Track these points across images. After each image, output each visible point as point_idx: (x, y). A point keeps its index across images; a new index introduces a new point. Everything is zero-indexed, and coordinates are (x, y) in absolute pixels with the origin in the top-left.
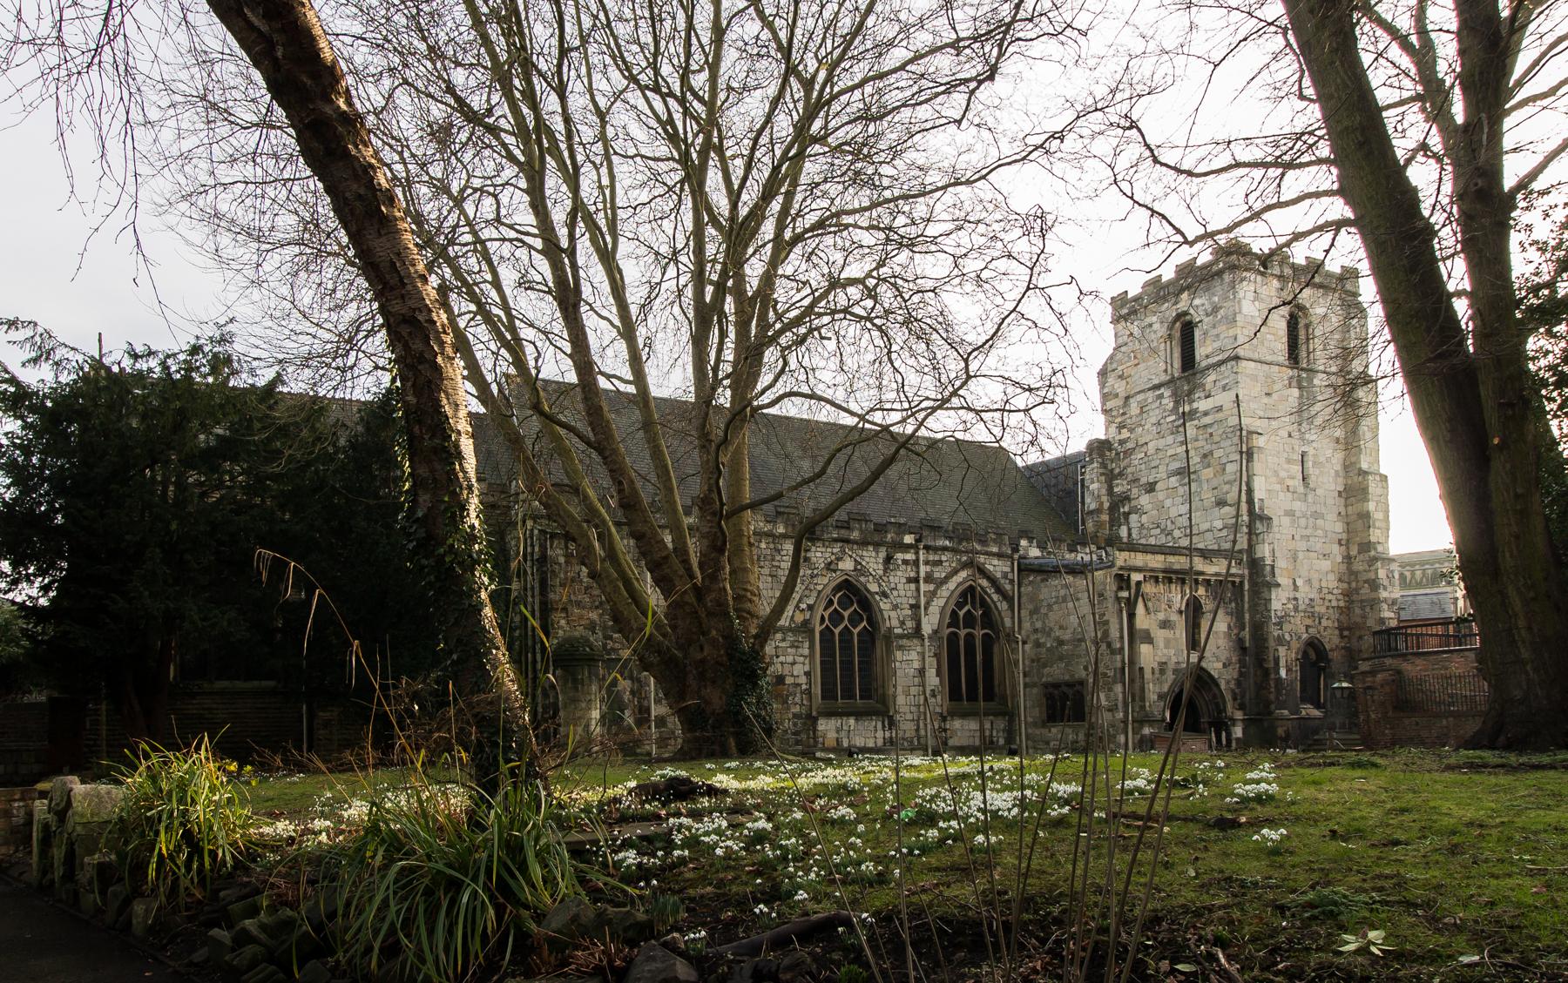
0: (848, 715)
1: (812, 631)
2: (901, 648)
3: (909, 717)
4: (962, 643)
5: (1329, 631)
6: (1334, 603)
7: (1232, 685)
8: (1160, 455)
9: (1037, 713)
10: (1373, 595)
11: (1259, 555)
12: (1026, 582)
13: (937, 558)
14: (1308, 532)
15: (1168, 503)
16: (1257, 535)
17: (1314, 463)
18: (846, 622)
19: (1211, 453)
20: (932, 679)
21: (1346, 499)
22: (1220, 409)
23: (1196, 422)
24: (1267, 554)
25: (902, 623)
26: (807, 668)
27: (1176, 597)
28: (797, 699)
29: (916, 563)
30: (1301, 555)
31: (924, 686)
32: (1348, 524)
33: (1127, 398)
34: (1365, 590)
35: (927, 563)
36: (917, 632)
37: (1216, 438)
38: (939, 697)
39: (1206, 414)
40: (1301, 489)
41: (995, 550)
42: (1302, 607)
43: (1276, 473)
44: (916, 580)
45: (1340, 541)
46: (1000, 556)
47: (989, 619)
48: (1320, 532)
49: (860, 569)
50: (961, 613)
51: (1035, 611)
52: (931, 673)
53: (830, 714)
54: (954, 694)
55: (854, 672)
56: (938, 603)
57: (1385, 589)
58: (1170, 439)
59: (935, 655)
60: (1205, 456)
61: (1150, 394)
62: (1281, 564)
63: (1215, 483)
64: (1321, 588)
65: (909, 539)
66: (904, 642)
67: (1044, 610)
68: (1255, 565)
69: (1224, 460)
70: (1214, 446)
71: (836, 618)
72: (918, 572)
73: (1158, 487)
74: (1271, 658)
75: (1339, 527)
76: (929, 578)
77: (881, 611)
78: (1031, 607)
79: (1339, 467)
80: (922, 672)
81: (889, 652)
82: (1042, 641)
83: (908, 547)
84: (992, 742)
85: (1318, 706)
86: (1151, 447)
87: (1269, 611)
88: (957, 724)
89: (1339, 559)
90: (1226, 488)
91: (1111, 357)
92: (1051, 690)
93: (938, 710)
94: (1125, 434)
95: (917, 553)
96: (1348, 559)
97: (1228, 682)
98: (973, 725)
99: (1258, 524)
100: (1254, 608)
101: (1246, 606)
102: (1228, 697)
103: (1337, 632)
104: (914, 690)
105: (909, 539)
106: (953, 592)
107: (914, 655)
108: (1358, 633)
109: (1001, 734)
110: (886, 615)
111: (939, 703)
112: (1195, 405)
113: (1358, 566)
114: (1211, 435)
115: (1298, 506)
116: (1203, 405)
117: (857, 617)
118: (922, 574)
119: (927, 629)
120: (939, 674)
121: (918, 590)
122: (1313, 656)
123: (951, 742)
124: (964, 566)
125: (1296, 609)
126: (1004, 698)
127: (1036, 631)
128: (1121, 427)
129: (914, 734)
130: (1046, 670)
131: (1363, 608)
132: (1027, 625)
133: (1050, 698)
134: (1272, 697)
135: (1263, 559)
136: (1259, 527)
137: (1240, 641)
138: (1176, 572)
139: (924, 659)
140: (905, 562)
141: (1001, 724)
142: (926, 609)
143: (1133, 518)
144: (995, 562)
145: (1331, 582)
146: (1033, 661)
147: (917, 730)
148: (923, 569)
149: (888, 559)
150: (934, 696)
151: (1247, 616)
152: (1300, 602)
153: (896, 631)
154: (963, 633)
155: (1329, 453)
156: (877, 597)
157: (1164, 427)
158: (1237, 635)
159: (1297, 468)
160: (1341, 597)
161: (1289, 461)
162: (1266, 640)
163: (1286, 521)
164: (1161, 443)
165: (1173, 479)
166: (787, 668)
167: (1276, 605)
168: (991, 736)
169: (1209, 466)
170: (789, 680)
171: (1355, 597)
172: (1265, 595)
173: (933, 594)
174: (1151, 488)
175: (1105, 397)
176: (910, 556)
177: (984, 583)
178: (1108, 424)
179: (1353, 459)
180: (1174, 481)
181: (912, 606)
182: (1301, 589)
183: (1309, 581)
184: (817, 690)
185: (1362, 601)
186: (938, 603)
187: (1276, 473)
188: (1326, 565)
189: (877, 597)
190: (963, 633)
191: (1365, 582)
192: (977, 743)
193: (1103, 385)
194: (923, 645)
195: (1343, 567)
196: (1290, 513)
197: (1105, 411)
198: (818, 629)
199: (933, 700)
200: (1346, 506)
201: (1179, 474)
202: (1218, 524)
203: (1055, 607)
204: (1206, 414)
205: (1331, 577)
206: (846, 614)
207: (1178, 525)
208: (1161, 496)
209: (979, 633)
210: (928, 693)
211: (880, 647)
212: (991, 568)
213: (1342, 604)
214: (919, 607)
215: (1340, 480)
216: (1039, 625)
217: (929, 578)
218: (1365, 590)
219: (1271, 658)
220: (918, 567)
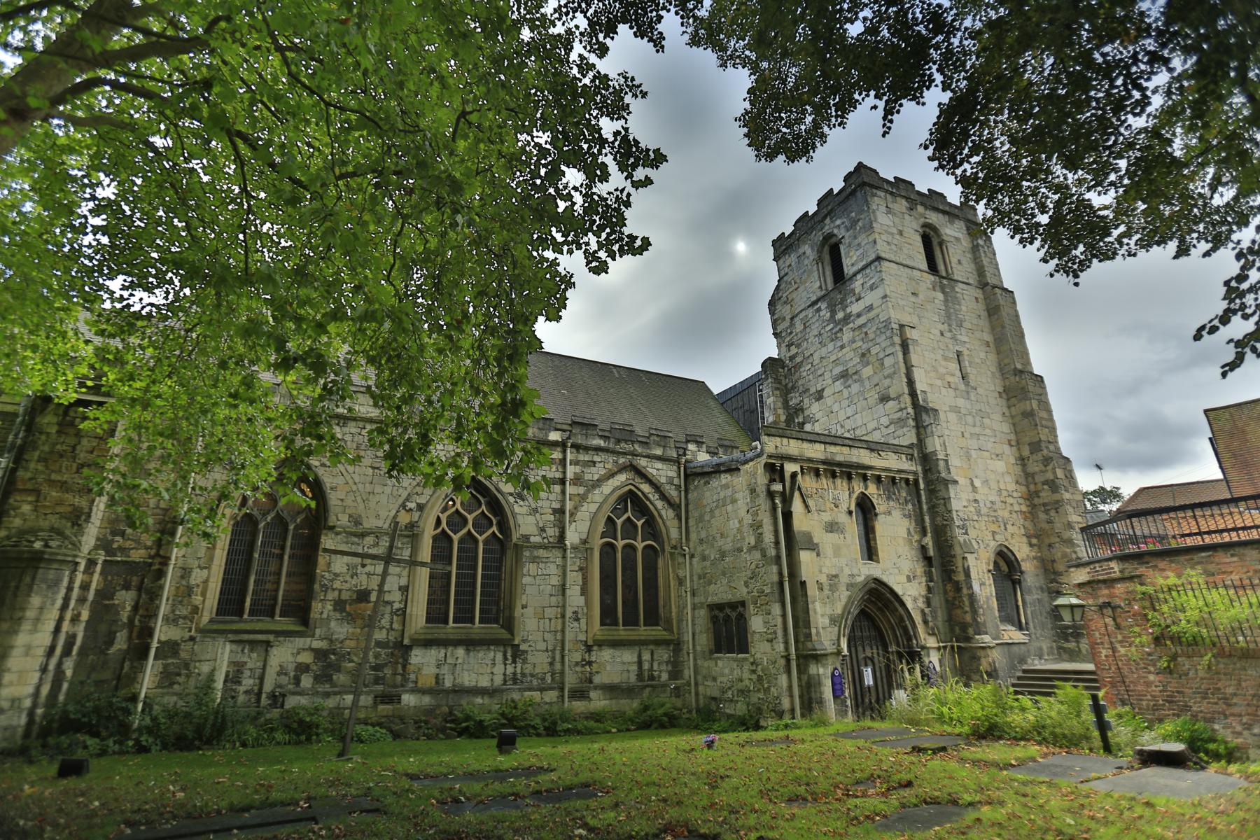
2: (535, 560)
3: (542, 646)
4: (619, 555)
5: (1017, 538)
6: (1016, 508)
7: (921, 604)
8: (825, 362)
9: (704, 640)
10: (1056, 497)
11: (930, 449)
12: (692, 487)
13: (587, 458)
14: (977, 430)
15: (836, 408)
16: (925, 428)
17: (970, 363)
18: (470, 526)
19: (869, 350)
20: (575, 598)
21: (1008, 400)
22: (870, 308)
23: (851, 325)
24: (938, 448)
25: (543, 530)
27: (843, 494)
29: (563, 462)
30: (973, 453)
31: (564, 606)
32: (1014, 425)
33: (792, 319)
34: (1046, 495)
35: (575, 463)
37: (871, 336)
38: (583, 621)
39: (859, 315)
40: (962, 387)
42: (984, 511)
43: (935, 369)
44: (562, 482)
45: (1009, 441)
47: (652, 528)
48: (988, 431)
50: (619, 522)
51: (700, 519)
54: (608, 616)
55: (474, 585)
56: (588, 509)
57: (1067, 491)
58: (831, 346)
59: (581, 569)
60: (863, 355)
61: (810, 312)
62: (955, 462)
63: (876, 380)
64: (1000, 490)
66: (541, 552)
67: (707, 518)
68: (927, 460)
69: (881, 355)
70: (871, 344)
72: (564, 473)
73: (826, 394)
74: (960, 569)
75: (1006, 428)
76: (577, 480)
77: (513, 513)
78: (696, 514)
79: (993, 369)
80: (563, 588)
82: (707, 552)
84: (652, 678)
85: (1021, 629)
86: (816, 356)
87: (950, 511)
88: (605, 655)
89: (1012, 461)
90: (887, 382)
91: (777, 288)
92: (716, 612)
93: (582, 637)
94: (794, 350)
95: (564, 452)
96: (1022, 460)
97: (915, 600)
98: (629, 656)
99: (924, 417)
100: (933, 508)
101: (925, 507)
102: (918, 618)
103: (1025, 539)
104: (550, 613)
105: (554, 436)
106: (607, 497)
107: (553, 569)
108: (1047, 541)
109: (664, 667)
110: (520, 519)
112: (848, 310)
113: (1034, 467)
114: (866, 333)
115: (961, 402)
116: (855, 308)
117: (484, 522)
118: (570, 475)
119: (572, 537)
120: (584, 591)
121: (563, 492)
122: (1005, 568)
123: (597, 680)
124: (622, 469)
125: (979, 513)
126: (669, 621)
127: (701, 541)
128: (789, 346)
129: (547, 668)
130: (712, 588)
131: (1047, 512)
132: (693, 536)
133: (714, 620)
134: (968, 618)
135: (934, 453)
136: (926, 419)
137: (923, 549)
138: (840, 464)
139: (564, 575)
141: (664, 654)
142: (572, 515)
145: (1009, 484)
146: (700, 578)
147: (551, 664)
148: (571, 471)
150: (577, 619)
151: (927, 518)
152: (982, 505)
153: (532, 539)
154: (620, 544)
155: (982, 355)
156: (511, 499)
157: (825, 335)
158: (919, 541)
159: (954, 366)
160: (1021, 501)
161: (946, 358)
162: (951, 546)
163: (952, 417)
164: (824, 351)
165: (837, 383)
167: (956, 505)
168: (651, 669)
169: (868, 364)
171: (1036, 501)
172: (942, 494)
173: (583, 498)
174: (819, 396)
175: (775, 323)
176: (557, 455)
177: (646, 488)
178: (779, 346)
179: (1006, 361)
180: (838, 385)
181: (555, 511)
182: (980, 490)
183: (986, 482)
185: (1044, 505)
186: (588, 509)
187: (935, 369)
188: (1000, 466)
189: (511, 499)
191: (1044, 483)
192: (633, 678)
193: (772, 313)
194: (564, 557)
195: (1018, 469)
196: (955, 409)
197: (775, 334)
199: (576, 624)
200: (1009, 407)
201: (843, 377)
202: (885, 421)
203: (717, 512)
204: (859, 315)
205: (1008, 479)
206: (470, 518)
207: (847, 427)
208: (828, 401)
209: (640, 545)
210: (569, 614)
211: (510, 554)
212: (654, 472)
213: (1024, 508)
214: (564, 513)
215: (999, 382)
216: (703, 535)
217: (577, 480)
218: (1046, 495)
219: (960, 569)
220: (564, 466)
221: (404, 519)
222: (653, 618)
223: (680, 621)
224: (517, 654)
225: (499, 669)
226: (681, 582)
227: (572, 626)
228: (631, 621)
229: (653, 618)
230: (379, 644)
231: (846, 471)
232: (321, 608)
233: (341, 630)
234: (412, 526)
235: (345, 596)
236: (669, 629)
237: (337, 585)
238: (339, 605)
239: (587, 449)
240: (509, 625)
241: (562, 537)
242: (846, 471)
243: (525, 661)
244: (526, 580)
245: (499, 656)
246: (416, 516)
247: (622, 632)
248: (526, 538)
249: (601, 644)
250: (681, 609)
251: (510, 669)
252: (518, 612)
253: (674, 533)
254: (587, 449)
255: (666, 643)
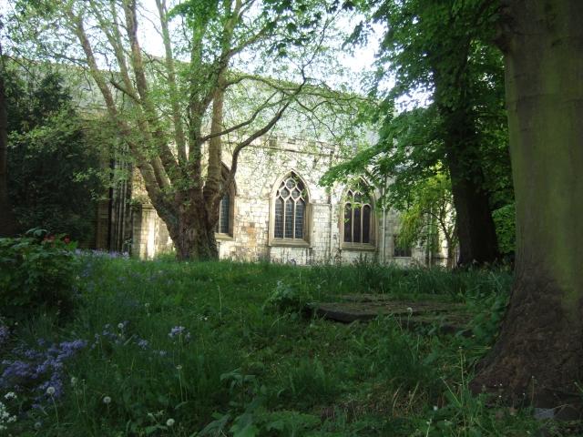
0: (288, 246)
2: (319, 211)
18: (291, 195)
20: (335, 229)
26: (267, 219)
28: (261, 235)
31: (330, 232)
49: (300, 165)
50: (354, 194)
52: (335, 225)
53: (277, 246)
54: (347, 237)
66: (322, 208)
80: (330, 225)
83: (325, 156)
93: (337, 246)
104: (325, 235)
117: (296, 193)
119: (334, 201)
120: (339, 226)
150: (335, 238)
166: (256, 219)
170: (257, 225)
184: (272, 231)
209: (362, 205)
221: (265, 191)
222: (366, 239)
223: (379, 241)
224: (311, 252)
225: (304, 258)
226: (380, 223)
227: (333, 241)
228: (357, 240)
229: (366, 239)
230: (259, 245)
232: (237, 230)
233: (245, 239)
235: (246, 225)
236: (374, 245)
237: (242, 220)
238: (243, 228)
240: (308, 239)
241: (329, 201)
243: (314, 255)
244: (315, 220)
245: (305, 252)
246: (270, 189)
247: (353, 244)
248: (314, 201)
249: (345, 249)
250: (380, 235)
251: (309, 258)
252: (312, 234)
255: (372, 251)
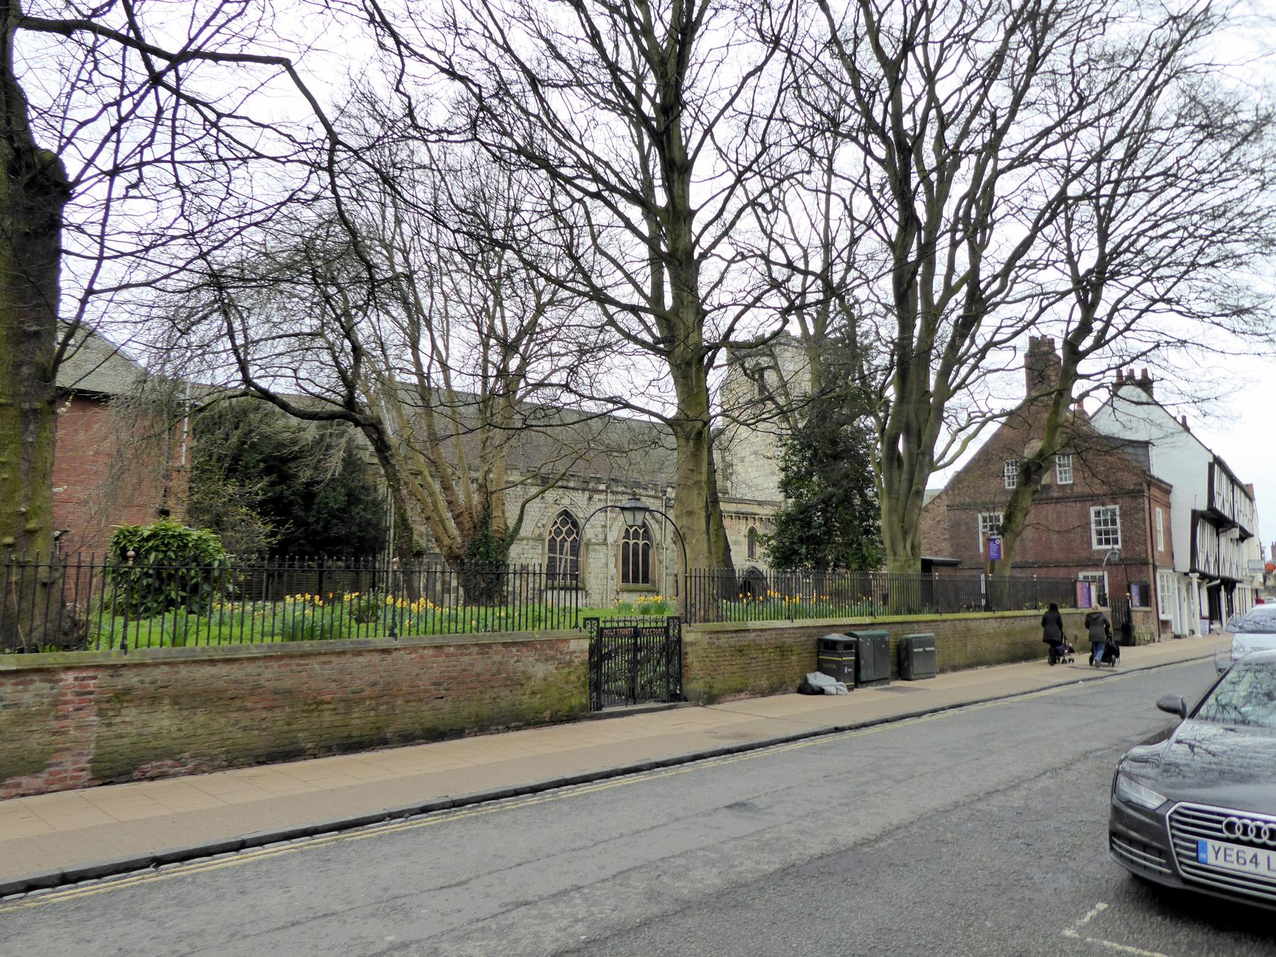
1: (544, 540)
2: (594, 550)
36: (605, 542)
41: (652, 493)
46: (655, 497)
47: (647, 535)
52: (612, 565)
54: (625, 578)
65: (602, 487)
71: (558, 532)
81: (587, 552)
104: (601, 576)
105: (602, 487)
107: (602, 555)
111: (617, 583)
119: (610, 540)
126: (654, 582)
140: (600, 500)
143: (734, 478)
144: (652, 500)
149: (590, 498)
154: (632, 542)
176: (603, 496)
190: (632, 542)
198: (548, 538)
209: (641, 543)
221: (537, 532)
222: (646, 580)
226: (661, 562)
227: (610, 582)
228: (636, 580)
231: (745, 516)
234: (540, 535)
239: (617, 493)
241: (605, 539)
242: (745, 516)
247: (631, 585)
249: (623, 591)
252: (587, 576)
253: (658, 537)
254: (617, 493)
